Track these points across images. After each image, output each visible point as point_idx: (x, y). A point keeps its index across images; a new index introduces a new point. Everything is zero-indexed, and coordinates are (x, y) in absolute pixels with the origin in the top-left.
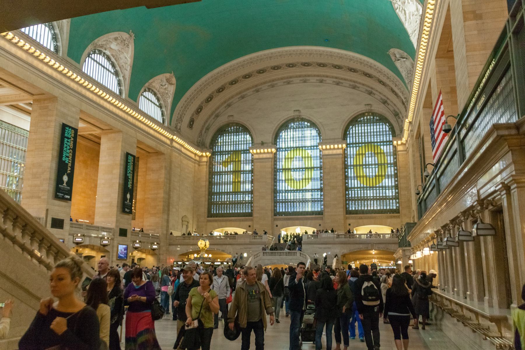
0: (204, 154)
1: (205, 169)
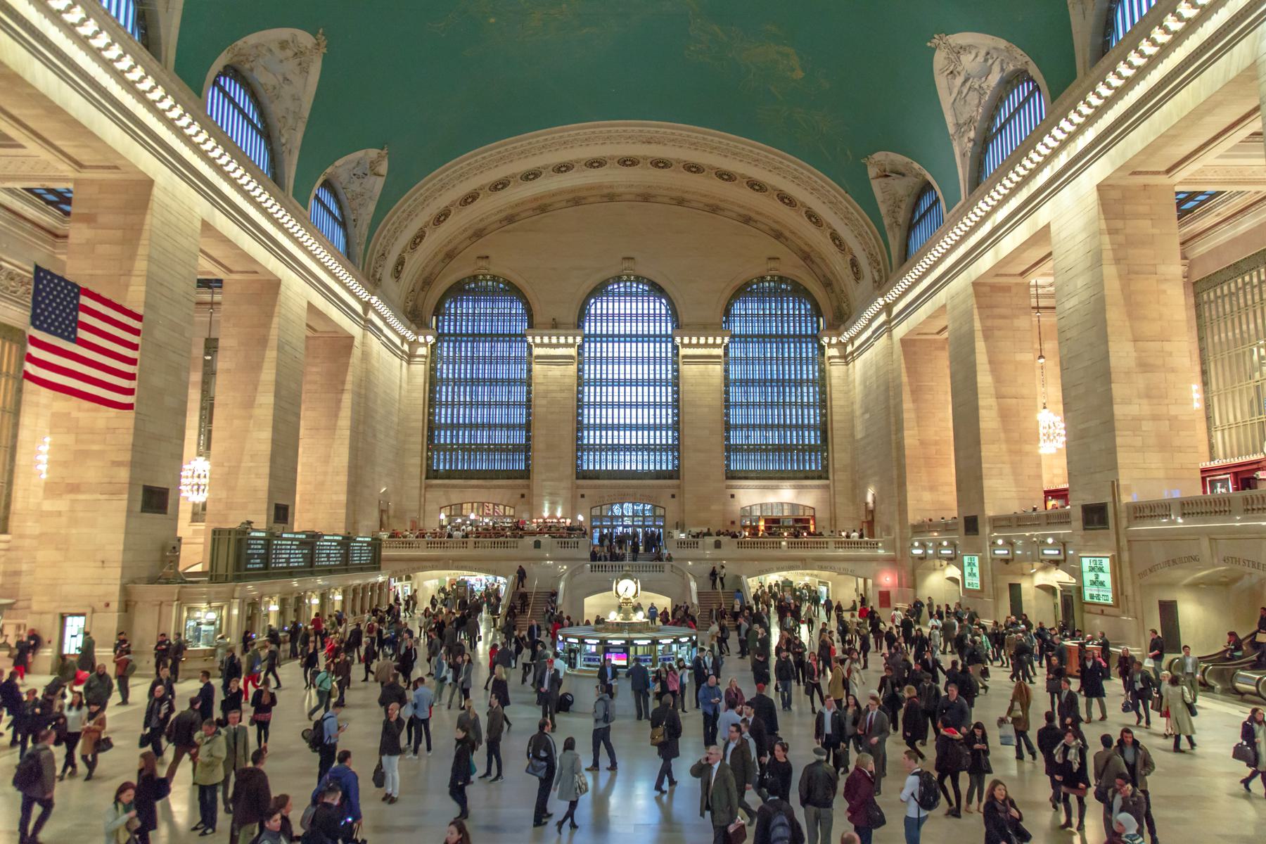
0: (421, 339)
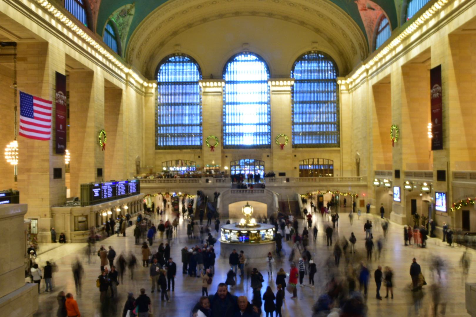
0: (150, 85)
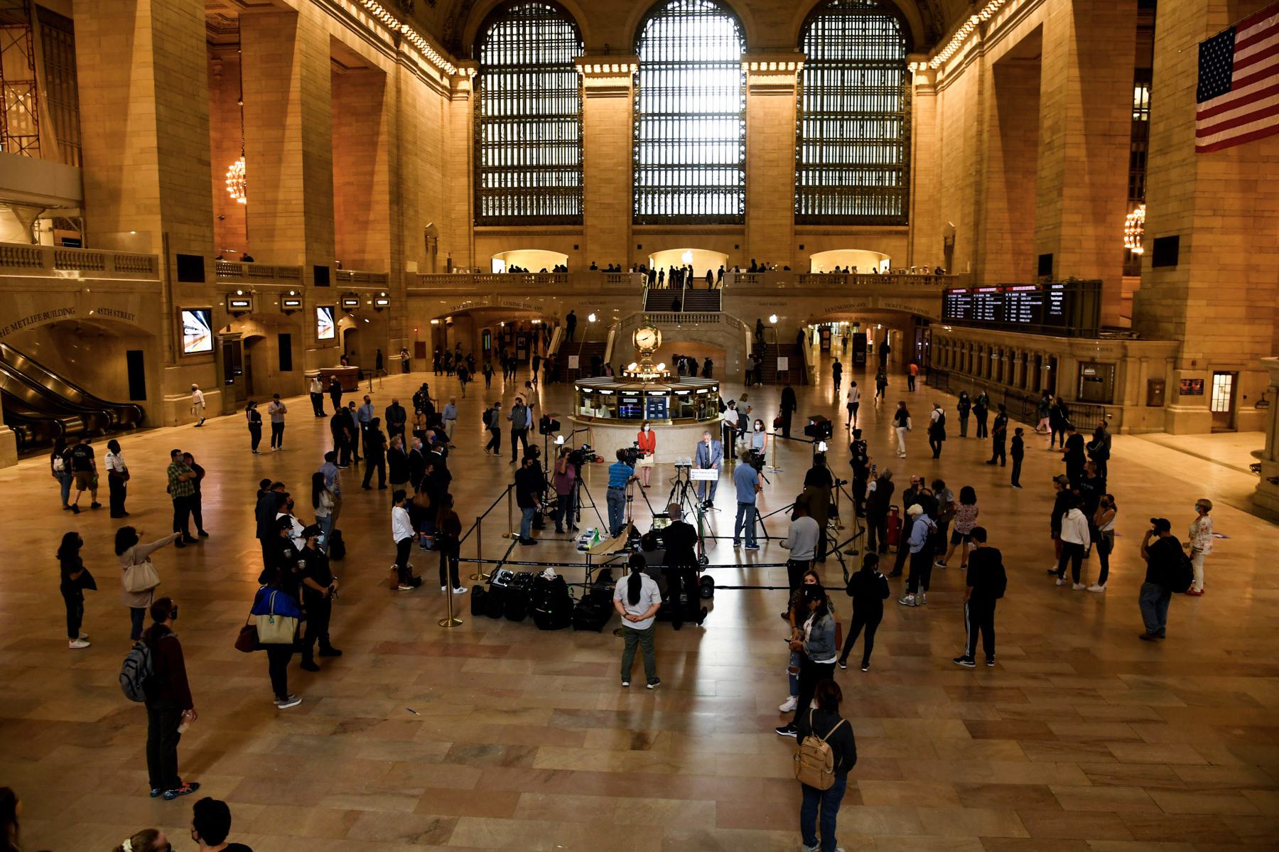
0: (462, 72)
1: (466, 111)
